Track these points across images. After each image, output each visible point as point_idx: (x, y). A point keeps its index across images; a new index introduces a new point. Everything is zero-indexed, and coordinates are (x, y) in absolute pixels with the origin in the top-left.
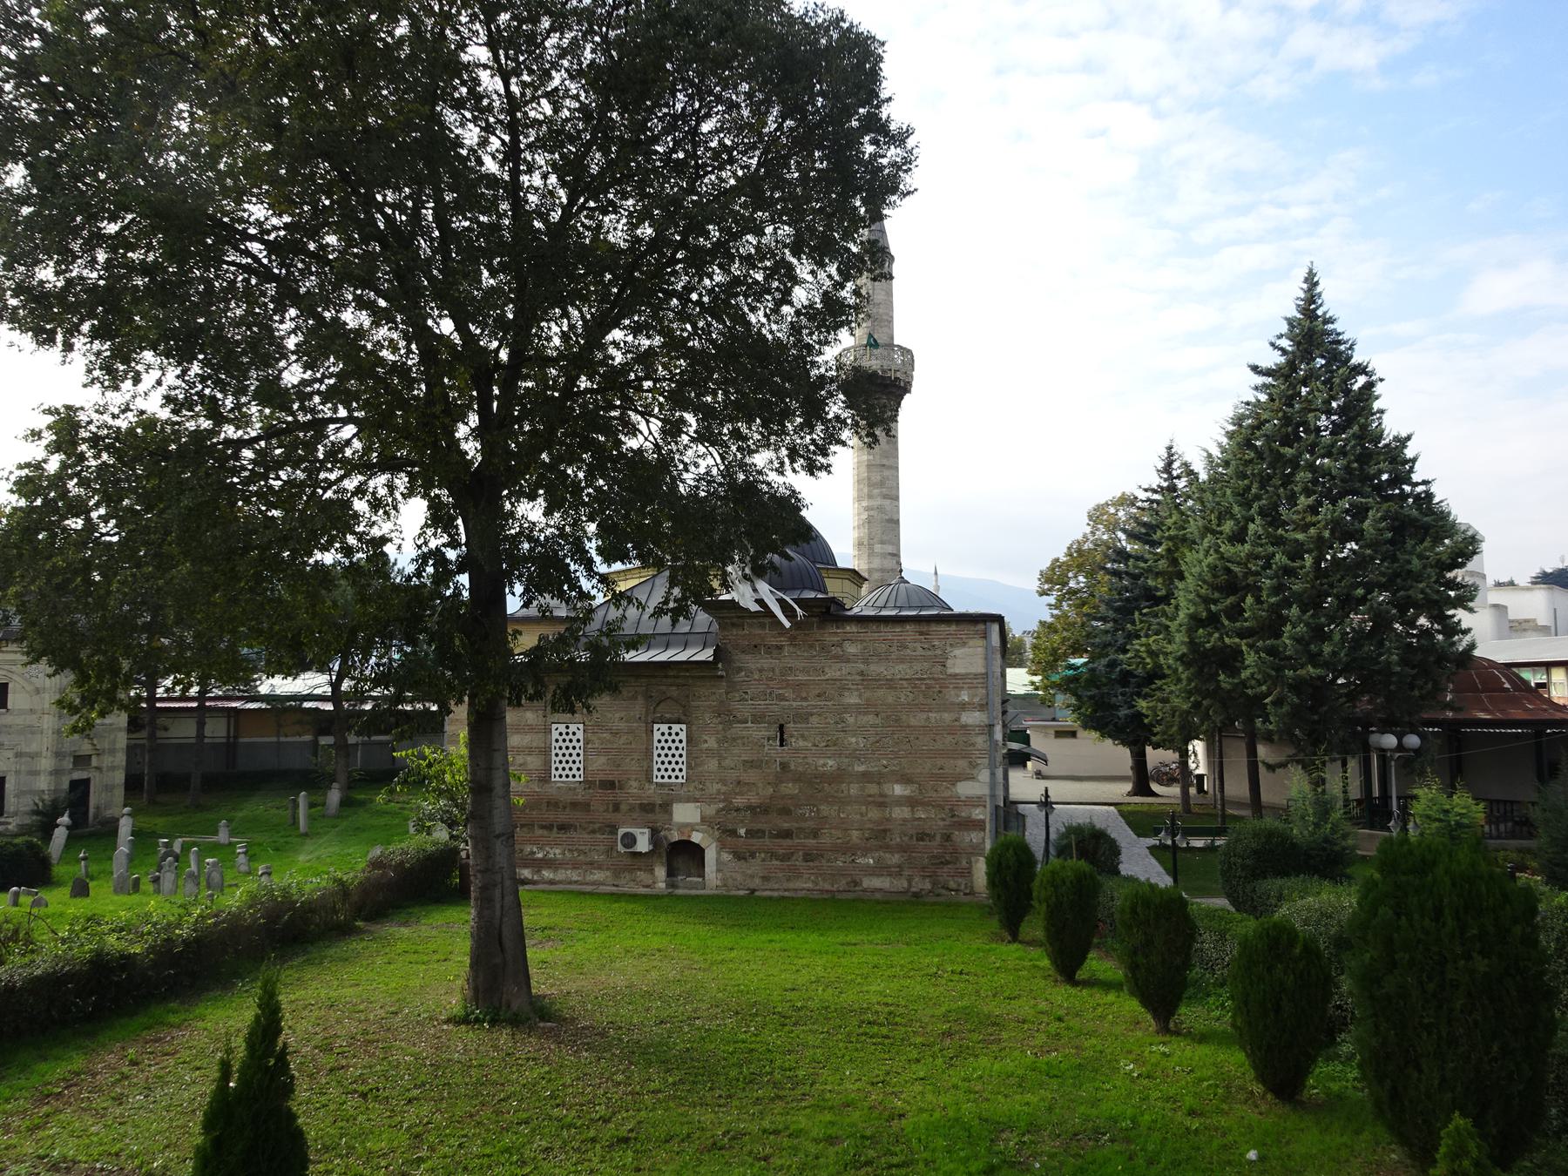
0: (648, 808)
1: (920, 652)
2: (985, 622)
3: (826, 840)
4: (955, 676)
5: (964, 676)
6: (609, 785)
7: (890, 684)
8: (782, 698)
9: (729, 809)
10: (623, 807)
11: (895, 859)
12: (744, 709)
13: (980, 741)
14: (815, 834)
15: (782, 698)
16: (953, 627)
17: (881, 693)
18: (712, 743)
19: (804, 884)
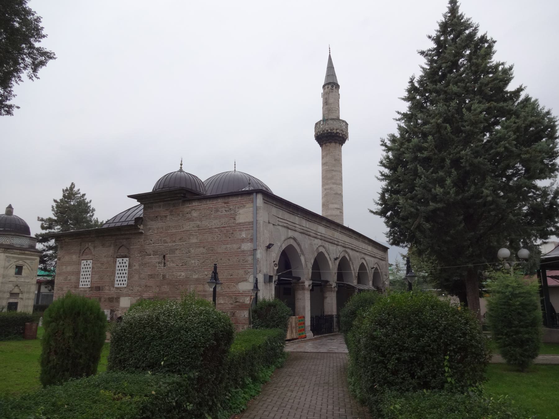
0: (111, 300)
1: (224, 213)
5: (244, 224)
6: (98, 289)
10: (103, 300)
16: (240, 198)
18: (137, 267)
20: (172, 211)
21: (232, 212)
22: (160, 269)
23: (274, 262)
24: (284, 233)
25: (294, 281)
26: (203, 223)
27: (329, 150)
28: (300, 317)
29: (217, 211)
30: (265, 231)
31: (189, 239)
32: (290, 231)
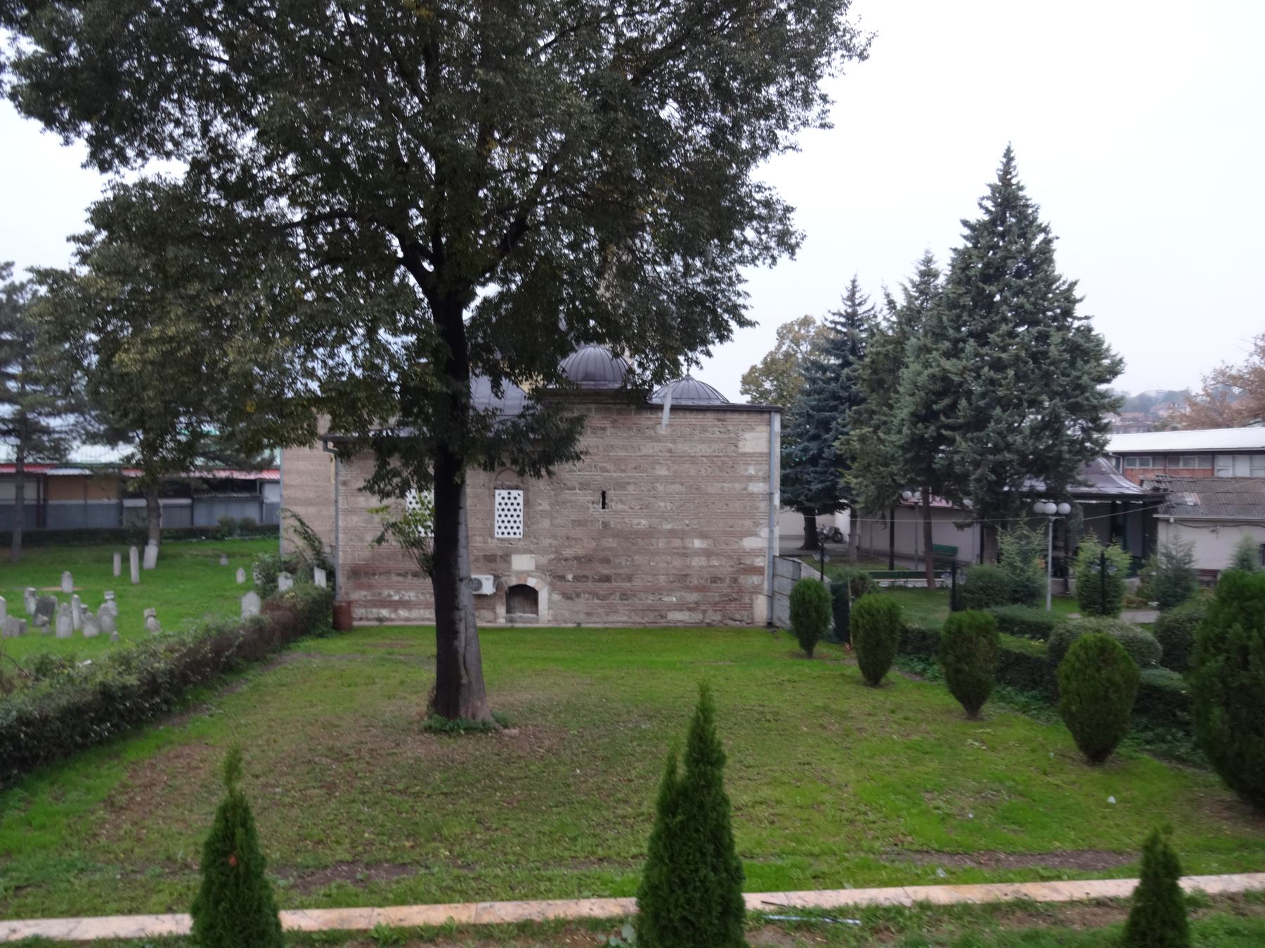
0: (490, 558)
2: (769, 412)
3: (638, 583)
4: (745, 454)
7: (693, 460)
8: (604, 470)
9: (558, 559)
11: (693, 597)
13: (763, 506)
14: (629, 578)
15: (604, 470)
17: (686, 466)
18: (545, 506)
19: (621, 618)
20: (614, 421)
26: (679, 446)
29: (704, 430)
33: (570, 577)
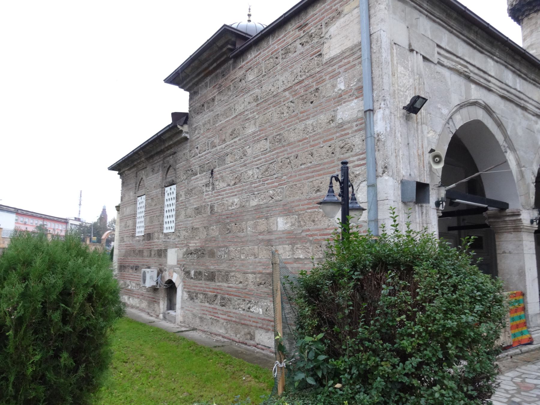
10: (153, 253)
12: (195, 163)
14: (226, 277)
21: (316, 40)
22: (209, 196)
23: (432, 151)
24: (457, 90)
25: (492, 210)
27: (536, 23)
28: (515, 295)
29: (287, 52)
30: (400, 69)
31: (244, 128)
32: (473, 86)
33: (192, 273)
